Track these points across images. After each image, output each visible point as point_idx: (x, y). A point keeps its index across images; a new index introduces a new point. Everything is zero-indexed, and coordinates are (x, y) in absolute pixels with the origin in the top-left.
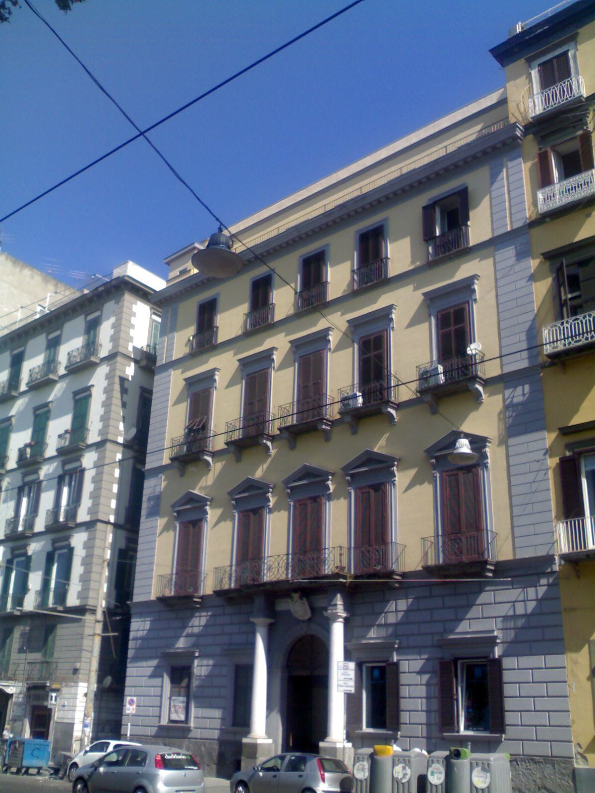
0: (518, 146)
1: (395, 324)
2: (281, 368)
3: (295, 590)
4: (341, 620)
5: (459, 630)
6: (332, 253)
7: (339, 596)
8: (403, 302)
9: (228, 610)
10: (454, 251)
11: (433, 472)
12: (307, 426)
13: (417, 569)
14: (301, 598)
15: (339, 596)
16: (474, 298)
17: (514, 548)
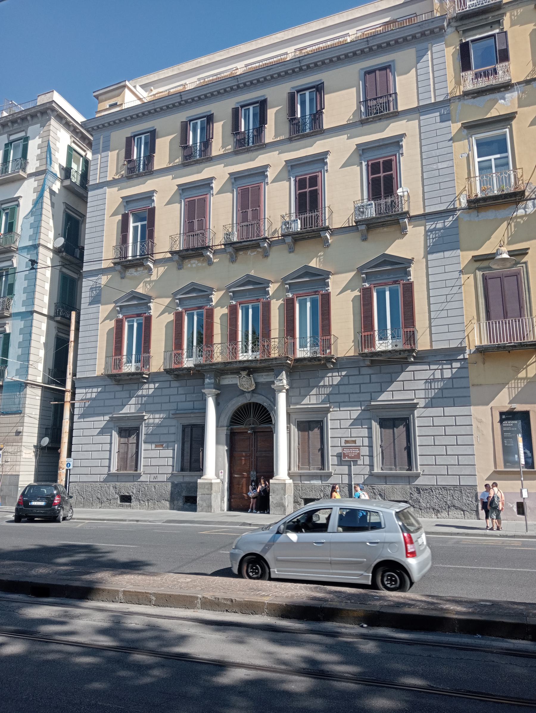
0: (443, 36)
1: (329, 167)
2: (219, 192)
3: (244, 369)
4: (284, 391)
5: (380, 399)
6: (398, 66)
7: (284, 372)
8: (338, 149)
9: (175, 384)
10: (385, 113)
11: (363, 284)
12: (247, 244)
13: (346, 355)
14: (248, 375)
15: (284, 372)
16: (401, 152)
17: (431, 341)
